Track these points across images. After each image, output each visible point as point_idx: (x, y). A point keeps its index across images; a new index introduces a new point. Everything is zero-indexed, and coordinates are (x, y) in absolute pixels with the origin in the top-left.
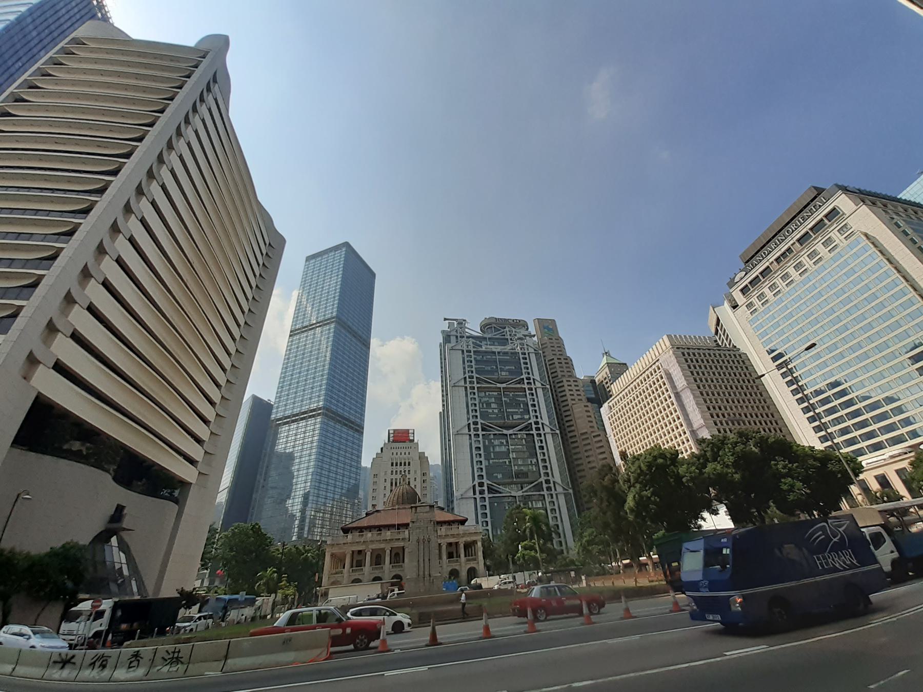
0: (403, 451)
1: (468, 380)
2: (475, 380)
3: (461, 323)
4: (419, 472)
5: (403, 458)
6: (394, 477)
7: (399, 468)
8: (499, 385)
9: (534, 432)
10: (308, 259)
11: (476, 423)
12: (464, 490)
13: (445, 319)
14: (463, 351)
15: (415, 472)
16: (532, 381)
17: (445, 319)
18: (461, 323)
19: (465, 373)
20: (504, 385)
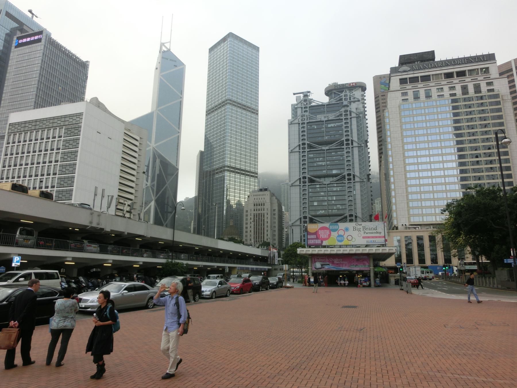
0: (261, 197)
1: (301, 146)
2: (306, 146)
3: (306, 95)
4: (269, 209)
5: (260, 201)
6: (255, 212)
7: (258, 207)
8: (324, 148)
9: (347, 181)
10: (211, 50)
11: (304, 178)
12: (294, 221)
13: (294, 94)
14: (299, 124)
15: (267, 209)
16: (350, 142)
17: (294, 94)
18: (306, 95)
19: (299, 140)
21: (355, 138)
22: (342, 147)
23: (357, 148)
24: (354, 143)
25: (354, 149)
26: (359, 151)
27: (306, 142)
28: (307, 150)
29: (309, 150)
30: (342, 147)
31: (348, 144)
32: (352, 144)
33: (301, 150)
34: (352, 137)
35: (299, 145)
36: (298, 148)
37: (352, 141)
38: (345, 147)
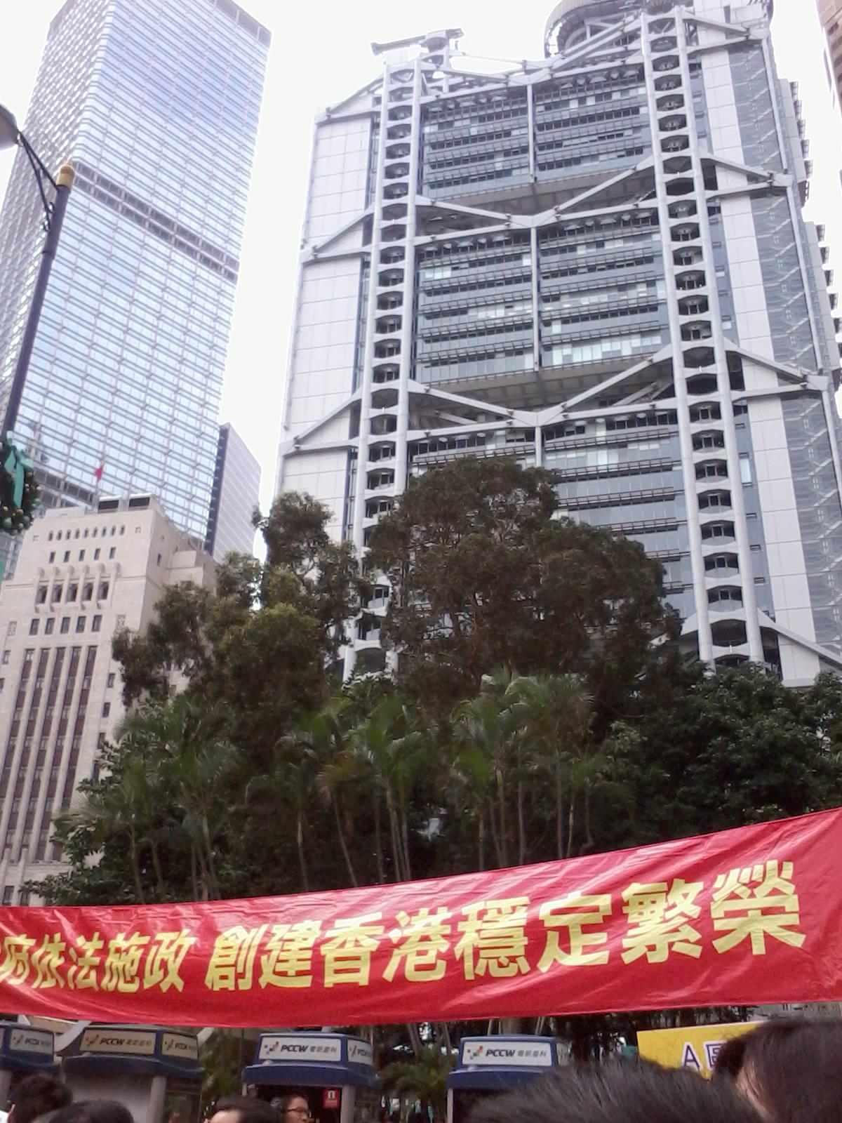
1: (368, 413)
8: (523, 419)
16: (719, 369)
20: (552, 415)
21: (756, 338)
22: (664, 404)
23: (775, 409)
24: (748, 372)
25: (755, 413)
26: (793, 433)
27: (403, 385)
28: (401, 437)
29: (418, 434)
30: (664, 404)
31: (702, 385)
32: (737, 381)
33: (364, 441)
34: (732, 334)
35: (355, 409)
36: (345, 424)
37: (735, 360)
38: (682, 401)
